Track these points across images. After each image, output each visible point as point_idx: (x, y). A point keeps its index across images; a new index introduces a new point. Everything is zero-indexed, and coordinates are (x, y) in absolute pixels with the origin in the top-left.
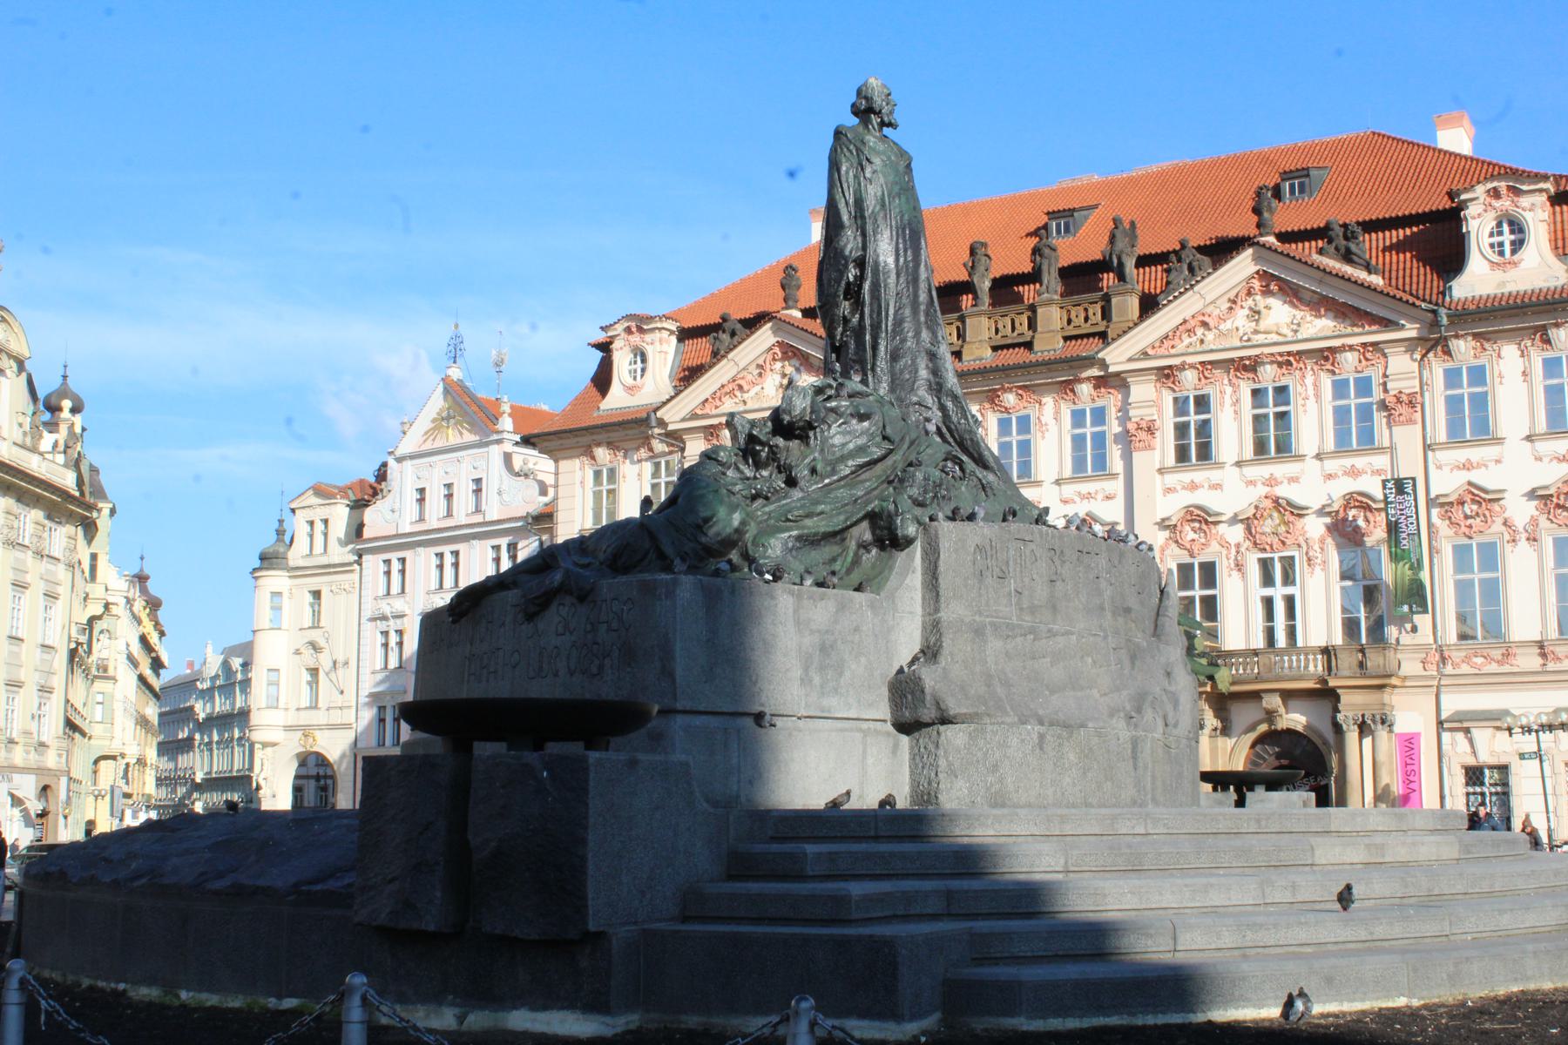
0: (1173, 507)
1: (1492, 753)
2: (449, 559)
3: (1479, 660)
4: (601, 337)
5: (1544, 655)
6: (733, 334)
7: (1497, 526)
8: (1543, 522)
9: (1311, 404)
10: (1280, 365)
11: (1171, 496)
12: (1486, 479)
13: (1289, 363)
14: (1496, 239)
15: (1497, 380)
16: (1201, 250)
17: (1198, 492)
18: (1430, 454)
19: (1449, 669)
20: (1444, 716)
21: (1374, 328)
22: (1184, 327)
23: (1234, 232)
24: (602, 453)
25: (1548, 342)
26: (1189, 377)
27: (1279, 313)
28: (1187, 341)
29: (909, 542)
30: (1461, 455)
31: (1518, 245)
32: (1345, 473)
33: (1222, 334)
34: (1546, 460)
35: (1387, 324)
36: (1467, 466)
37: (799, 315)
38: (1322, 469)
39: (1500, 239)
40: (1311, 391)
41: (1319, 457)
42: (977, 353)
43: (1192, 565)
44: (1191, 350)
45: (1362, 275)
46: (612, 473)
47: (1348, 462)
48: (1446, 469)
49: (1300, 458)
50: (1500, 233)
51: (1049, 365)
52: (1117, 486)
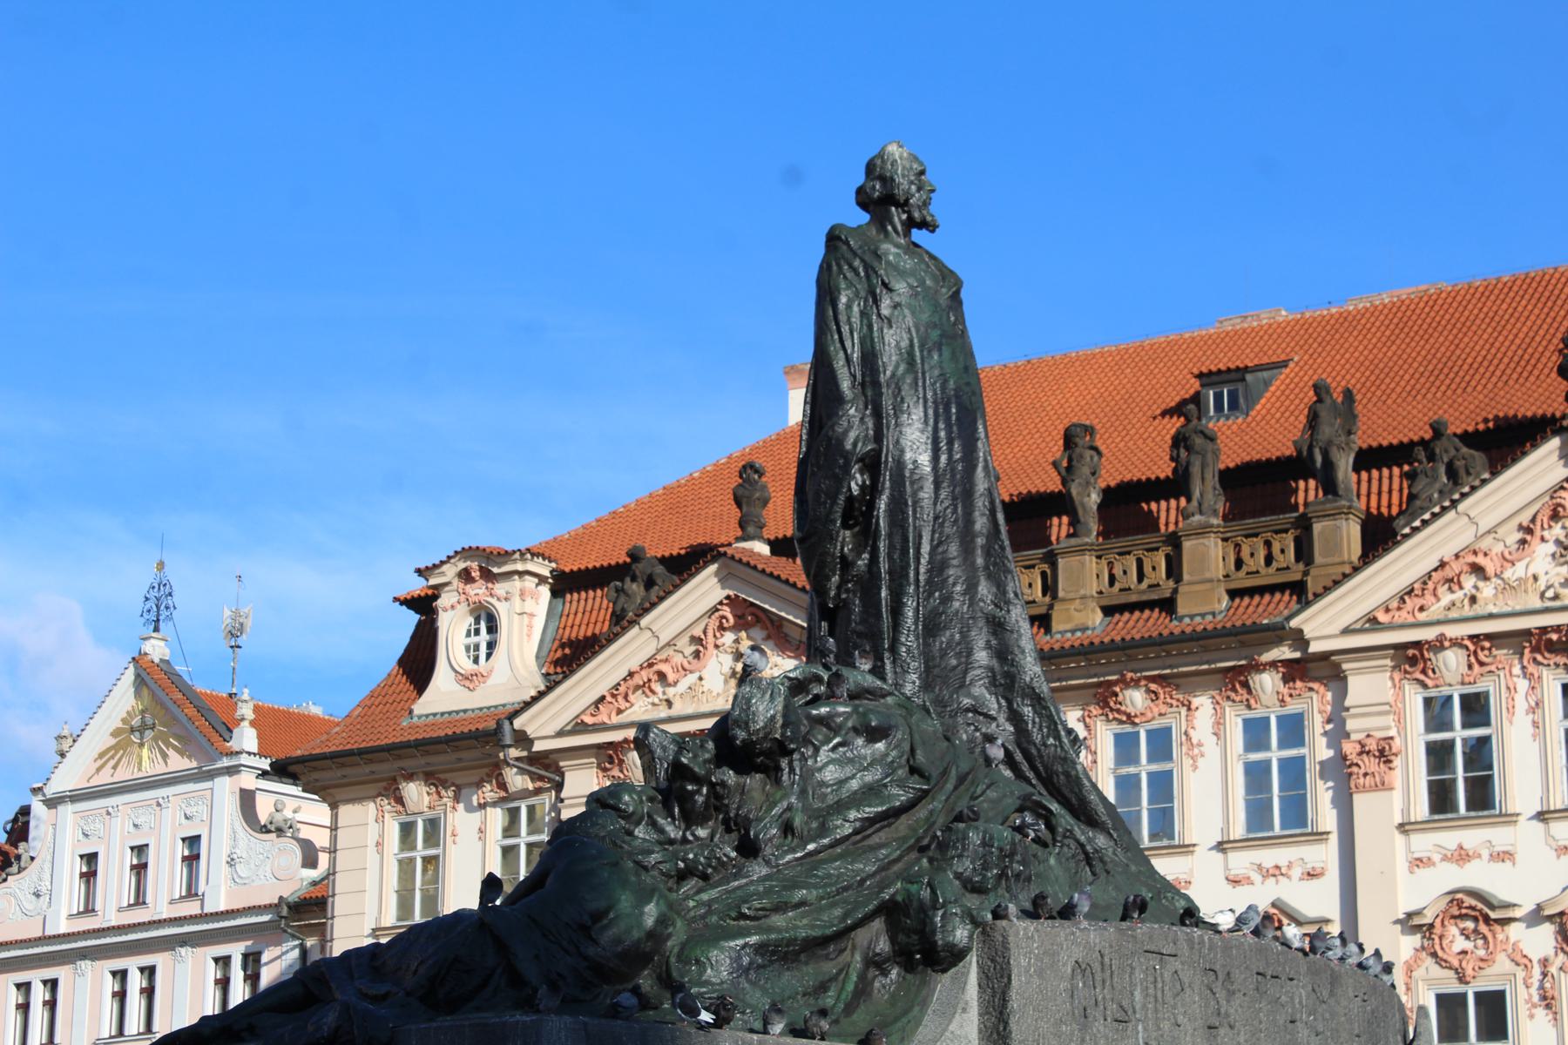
0: (1424, 891)
2: (136, 982)
4: (417, 586)
6: (650, 583)
11: (1422, 873)
15: (449, 839)
16: (1468, 438)
17: (1474, 865)
22: (1442, 575)
23: (1527, 407)
24: (415, 792)
26: (1452, 662)
28: (1447, 598)
29: (957, 955)
33: (1508, 587)
37: (763, 549)
42: (1078, 619)
43: (1464, 996)
44: (1454, 614)
46: (433, 827)
49: (1509, 818)
51: (1206, 640)
52: (1327, 855)
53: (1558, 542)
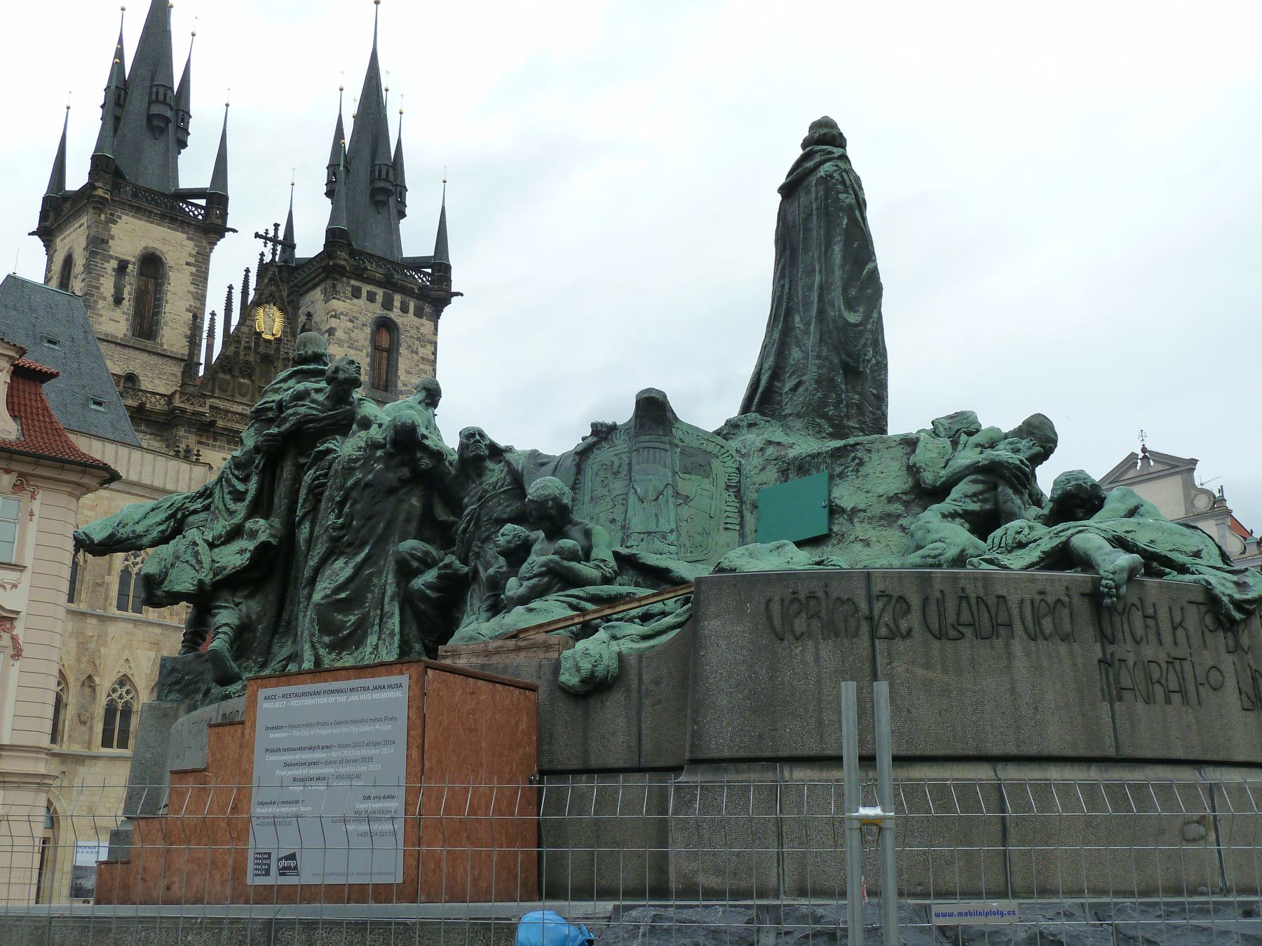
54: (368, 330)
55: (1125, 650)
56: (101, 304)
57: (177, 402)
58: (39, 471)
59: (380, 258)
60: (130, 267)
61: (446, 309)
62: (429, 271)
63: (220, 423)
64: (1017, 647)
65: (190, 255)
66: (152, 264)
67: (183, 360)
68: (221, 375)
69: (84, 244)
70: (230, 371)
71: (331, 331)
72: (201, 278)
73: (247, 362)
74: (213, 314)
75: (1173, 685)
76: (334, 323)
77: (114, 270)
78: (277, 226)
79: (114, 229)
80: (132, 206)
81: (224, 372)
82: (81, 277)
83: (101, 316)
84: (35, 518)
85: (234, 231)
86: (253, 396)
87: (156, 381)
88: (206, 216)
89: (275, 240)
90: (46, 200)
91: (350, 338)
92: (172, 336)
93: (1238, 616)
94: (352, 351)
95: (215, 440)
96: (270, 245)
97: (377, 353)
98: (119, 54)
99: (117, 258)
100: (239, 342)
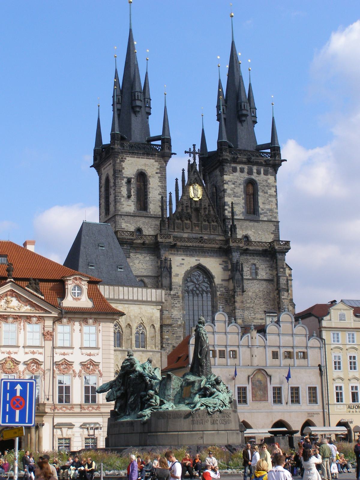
1: (67, 435)
3: (64, 409)
5: (81, 408)
7: (71, 372)
8: (83, 372)
9: (22, 331)
10: (14, 318)
12: (69, 358)
13: (17, 318)
14: (74, 291)
18: (54, 349)
19: (56, 411)
20: (54, 424)
21: (42, 311)
25: (87, 322)
27: (14, 302)
30: (63, 351)
31: (80, 294)
32: (31, 353)
34: (84, 355)
35: (46, 311)
36: (64, 354)
38: (24, 350)
39: (75, 291)
40: (22, 327)
41: (24, 347)
45: (40, 296)
47: (32, 350)
48: (58, 354)
50: (75, 290)
53: (6, 300)
54: (242, 187)
55: (195, 419)
56: (123, 199)
57: (160, 240)
58: (101, 317)
59: (245, 151)
60: (133, 180)
61: (280, 169)
62: (269, 151)
63: (179, 244)
64: (182, 419)
65: (157, 169)
66: (142, 176)
67: (160, 218)
68: (177, 221)
69: (112, 173)
70: (181, 219)
71: (224, 191)
72: (163, 178)
73: (188, 213)
74: (170, 194)
75: (201, 422)
76: (226, 186)
77: (126, 183)
78: (194, 145)
79: (124, 165)
80: (130, 153)
81: (178, 219)
82: (113, 188)
83: (123, 205)
84: (101, 332)
85: (175, 154)
86: (192, 228)
87: (150, 229)
88: (163, 149)
89: (194, 153)
90: (96, 152)
91: (234, 192)
92: (154, 207)
93: (211, 413)
94: (235, 199)
95: (178, 251)
96: (192, 155)
97: (248, 197)
98: (116, 77)
99: (126, 177)
100: (183, 204)
